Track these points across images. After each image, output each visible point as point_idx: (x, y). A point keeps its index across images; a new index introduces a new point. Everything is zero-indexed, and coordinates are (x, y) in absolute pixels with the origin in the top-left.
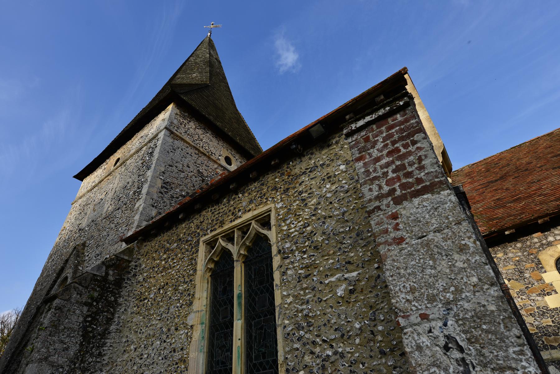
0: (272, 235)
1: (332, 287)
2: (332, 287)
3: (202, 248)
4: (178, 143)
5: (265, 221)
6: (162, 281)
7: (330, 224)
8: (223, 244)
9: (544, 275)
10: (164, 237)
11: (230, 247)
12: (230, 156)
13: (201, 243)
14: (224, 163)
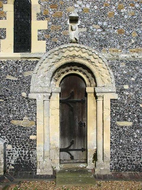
9: (4, 5)
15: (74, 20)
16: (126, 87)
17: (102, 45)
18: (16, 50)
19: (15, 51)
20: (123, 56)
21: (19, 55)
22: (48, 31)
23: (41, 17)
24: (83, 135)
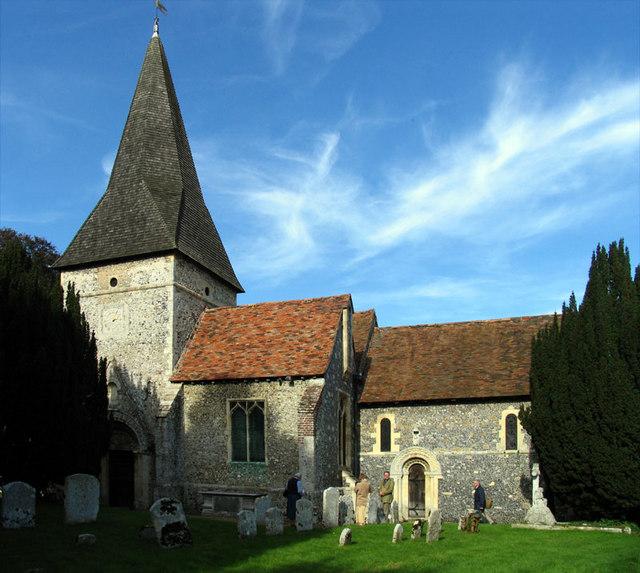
12: (209, 286)
14: (205, 297)
15: (416, 433)
16: (448, 472)
17: (434, 446)
18: (383, 449)
20: (446, 453)
21: (383, 453)
22: (400, 439)
23: (397, 431)
24: (423, 501)
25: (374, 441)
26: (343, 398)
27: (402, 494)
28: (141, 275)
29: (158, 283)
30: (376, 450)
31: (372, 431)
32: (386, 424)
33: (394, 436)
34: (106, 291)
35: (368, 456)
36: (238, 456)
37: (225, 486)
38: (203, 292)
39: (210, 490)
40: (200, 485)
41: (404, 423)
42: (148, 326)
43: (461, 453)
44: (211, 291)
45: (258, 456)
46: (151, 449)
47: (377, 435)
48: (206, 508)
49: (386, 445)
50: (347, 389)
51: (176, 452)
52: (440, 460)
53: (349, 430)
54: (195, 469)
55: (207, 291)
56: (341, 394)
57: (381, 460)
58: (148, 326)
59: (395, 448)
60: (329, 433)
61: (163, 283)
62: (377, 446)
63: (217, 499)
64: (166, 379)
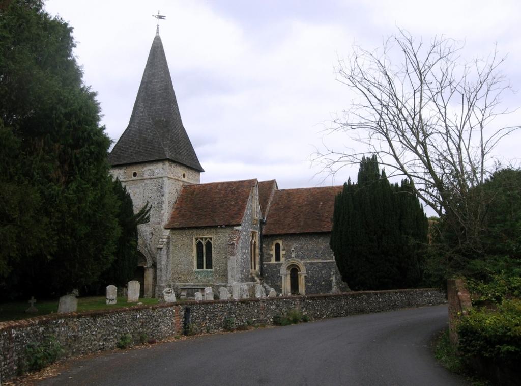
0: (212, 243)
1: (222, 256)
2: (222, 256)
3: (194, 240)
4: (171, 180)
5: (211, 239)
6: (182, 244)
7: (224, 246)
8: (200, 240)
10: (181, 231)
11: (202, 241)
13: (194, 239)
15: (293, 251)
17: (302, 258)
19: (276, 261)
20: (308, 261)
21: (277, 262)
22: (285, 254)
23: (283, 250)
25: (272, 256)
26: (253, 233)
27: (286, 284)
28: (150, 171)
29: (158, 176)
30: (273, 261)
31: (271, 250)
32: (278, 246)
33: (282, 253)
34: (131, 179)
35: (269, 264)
36: (200, 266)
37: (192, 284)
38: (182, 177)
39: (184, 286)
40: (179, 284)
41: (287, 246)
42: (153, 198)
43: (316, 261)
44: (186, 175)
45: (209, 266)
46: (154, 266)
47: (273, 252)
48: (182, 295)
49: (278, 259)
50: (255, 228)
51: (167, 266)
52: (305, 264)
53: (257, 251)
54: (176, 275)
55: (184, 176)
56: (252, 232)
57: (275, 266)
58: (153, 198)
59: (282, 259)
60: (244, 253)
61: (161, 176)
62: (273, 259)
63: (188, 291)
64: (162, 227)
